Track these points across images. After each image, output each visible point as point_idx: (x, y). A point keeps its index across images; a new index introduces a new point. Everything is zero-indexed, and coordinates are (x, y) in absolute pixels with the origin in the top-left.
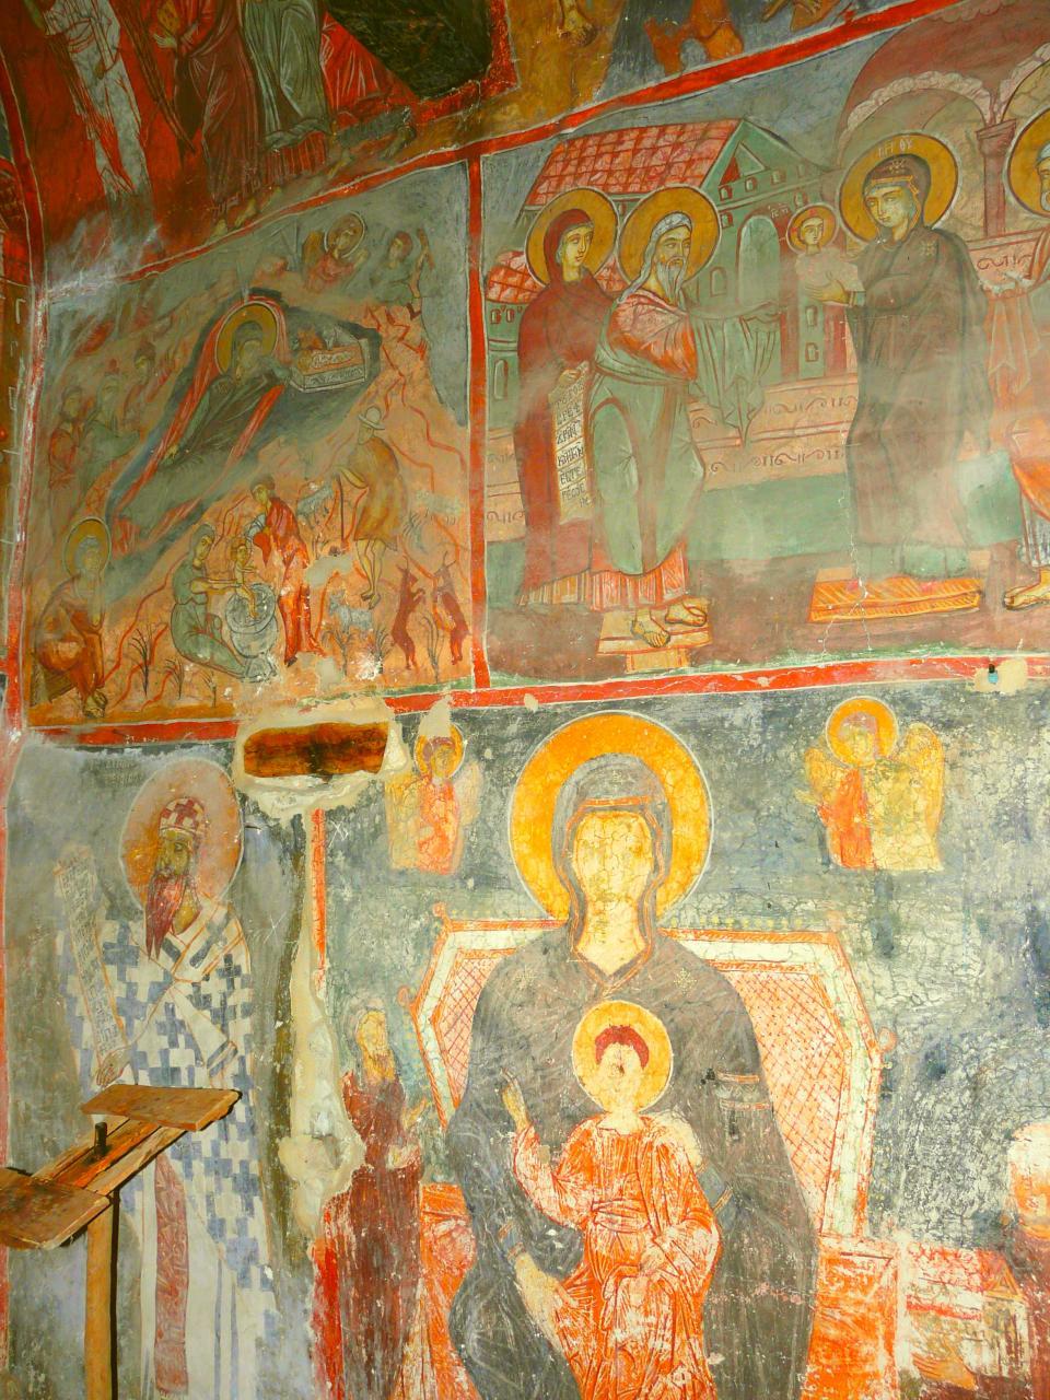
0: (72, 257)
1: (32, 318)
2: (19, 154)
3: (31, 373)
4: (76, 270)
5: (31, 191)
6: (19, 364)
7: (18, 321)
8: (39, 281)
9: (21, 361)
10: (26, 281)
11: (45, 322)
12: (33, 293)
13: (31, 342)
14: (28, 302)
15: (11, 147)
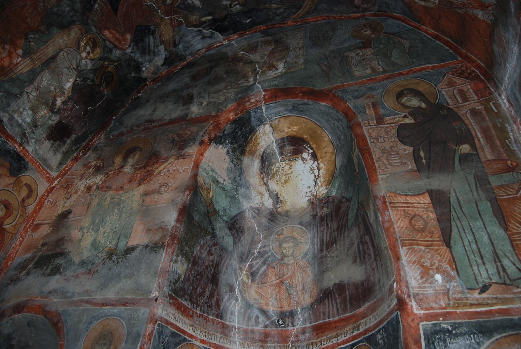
0: (500, 65)
1: (503, 105)
2: (460, 55)
3: (515, 127)
4: (505, 65)
5: (474, 61)
6: (506, 127)
7: (496, 111)
8: (497, 89)
9: (507, 125)
10: (491, 93)
11: (509, 102)
12: (497, 95)
13: (508, 115)
14: (497, 100)
15: (456, 55)
